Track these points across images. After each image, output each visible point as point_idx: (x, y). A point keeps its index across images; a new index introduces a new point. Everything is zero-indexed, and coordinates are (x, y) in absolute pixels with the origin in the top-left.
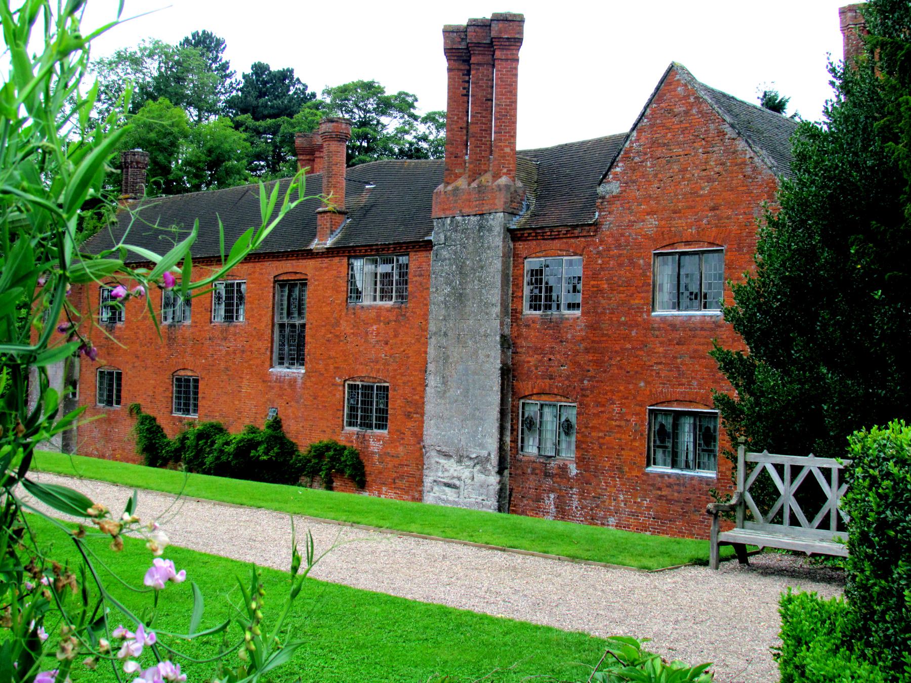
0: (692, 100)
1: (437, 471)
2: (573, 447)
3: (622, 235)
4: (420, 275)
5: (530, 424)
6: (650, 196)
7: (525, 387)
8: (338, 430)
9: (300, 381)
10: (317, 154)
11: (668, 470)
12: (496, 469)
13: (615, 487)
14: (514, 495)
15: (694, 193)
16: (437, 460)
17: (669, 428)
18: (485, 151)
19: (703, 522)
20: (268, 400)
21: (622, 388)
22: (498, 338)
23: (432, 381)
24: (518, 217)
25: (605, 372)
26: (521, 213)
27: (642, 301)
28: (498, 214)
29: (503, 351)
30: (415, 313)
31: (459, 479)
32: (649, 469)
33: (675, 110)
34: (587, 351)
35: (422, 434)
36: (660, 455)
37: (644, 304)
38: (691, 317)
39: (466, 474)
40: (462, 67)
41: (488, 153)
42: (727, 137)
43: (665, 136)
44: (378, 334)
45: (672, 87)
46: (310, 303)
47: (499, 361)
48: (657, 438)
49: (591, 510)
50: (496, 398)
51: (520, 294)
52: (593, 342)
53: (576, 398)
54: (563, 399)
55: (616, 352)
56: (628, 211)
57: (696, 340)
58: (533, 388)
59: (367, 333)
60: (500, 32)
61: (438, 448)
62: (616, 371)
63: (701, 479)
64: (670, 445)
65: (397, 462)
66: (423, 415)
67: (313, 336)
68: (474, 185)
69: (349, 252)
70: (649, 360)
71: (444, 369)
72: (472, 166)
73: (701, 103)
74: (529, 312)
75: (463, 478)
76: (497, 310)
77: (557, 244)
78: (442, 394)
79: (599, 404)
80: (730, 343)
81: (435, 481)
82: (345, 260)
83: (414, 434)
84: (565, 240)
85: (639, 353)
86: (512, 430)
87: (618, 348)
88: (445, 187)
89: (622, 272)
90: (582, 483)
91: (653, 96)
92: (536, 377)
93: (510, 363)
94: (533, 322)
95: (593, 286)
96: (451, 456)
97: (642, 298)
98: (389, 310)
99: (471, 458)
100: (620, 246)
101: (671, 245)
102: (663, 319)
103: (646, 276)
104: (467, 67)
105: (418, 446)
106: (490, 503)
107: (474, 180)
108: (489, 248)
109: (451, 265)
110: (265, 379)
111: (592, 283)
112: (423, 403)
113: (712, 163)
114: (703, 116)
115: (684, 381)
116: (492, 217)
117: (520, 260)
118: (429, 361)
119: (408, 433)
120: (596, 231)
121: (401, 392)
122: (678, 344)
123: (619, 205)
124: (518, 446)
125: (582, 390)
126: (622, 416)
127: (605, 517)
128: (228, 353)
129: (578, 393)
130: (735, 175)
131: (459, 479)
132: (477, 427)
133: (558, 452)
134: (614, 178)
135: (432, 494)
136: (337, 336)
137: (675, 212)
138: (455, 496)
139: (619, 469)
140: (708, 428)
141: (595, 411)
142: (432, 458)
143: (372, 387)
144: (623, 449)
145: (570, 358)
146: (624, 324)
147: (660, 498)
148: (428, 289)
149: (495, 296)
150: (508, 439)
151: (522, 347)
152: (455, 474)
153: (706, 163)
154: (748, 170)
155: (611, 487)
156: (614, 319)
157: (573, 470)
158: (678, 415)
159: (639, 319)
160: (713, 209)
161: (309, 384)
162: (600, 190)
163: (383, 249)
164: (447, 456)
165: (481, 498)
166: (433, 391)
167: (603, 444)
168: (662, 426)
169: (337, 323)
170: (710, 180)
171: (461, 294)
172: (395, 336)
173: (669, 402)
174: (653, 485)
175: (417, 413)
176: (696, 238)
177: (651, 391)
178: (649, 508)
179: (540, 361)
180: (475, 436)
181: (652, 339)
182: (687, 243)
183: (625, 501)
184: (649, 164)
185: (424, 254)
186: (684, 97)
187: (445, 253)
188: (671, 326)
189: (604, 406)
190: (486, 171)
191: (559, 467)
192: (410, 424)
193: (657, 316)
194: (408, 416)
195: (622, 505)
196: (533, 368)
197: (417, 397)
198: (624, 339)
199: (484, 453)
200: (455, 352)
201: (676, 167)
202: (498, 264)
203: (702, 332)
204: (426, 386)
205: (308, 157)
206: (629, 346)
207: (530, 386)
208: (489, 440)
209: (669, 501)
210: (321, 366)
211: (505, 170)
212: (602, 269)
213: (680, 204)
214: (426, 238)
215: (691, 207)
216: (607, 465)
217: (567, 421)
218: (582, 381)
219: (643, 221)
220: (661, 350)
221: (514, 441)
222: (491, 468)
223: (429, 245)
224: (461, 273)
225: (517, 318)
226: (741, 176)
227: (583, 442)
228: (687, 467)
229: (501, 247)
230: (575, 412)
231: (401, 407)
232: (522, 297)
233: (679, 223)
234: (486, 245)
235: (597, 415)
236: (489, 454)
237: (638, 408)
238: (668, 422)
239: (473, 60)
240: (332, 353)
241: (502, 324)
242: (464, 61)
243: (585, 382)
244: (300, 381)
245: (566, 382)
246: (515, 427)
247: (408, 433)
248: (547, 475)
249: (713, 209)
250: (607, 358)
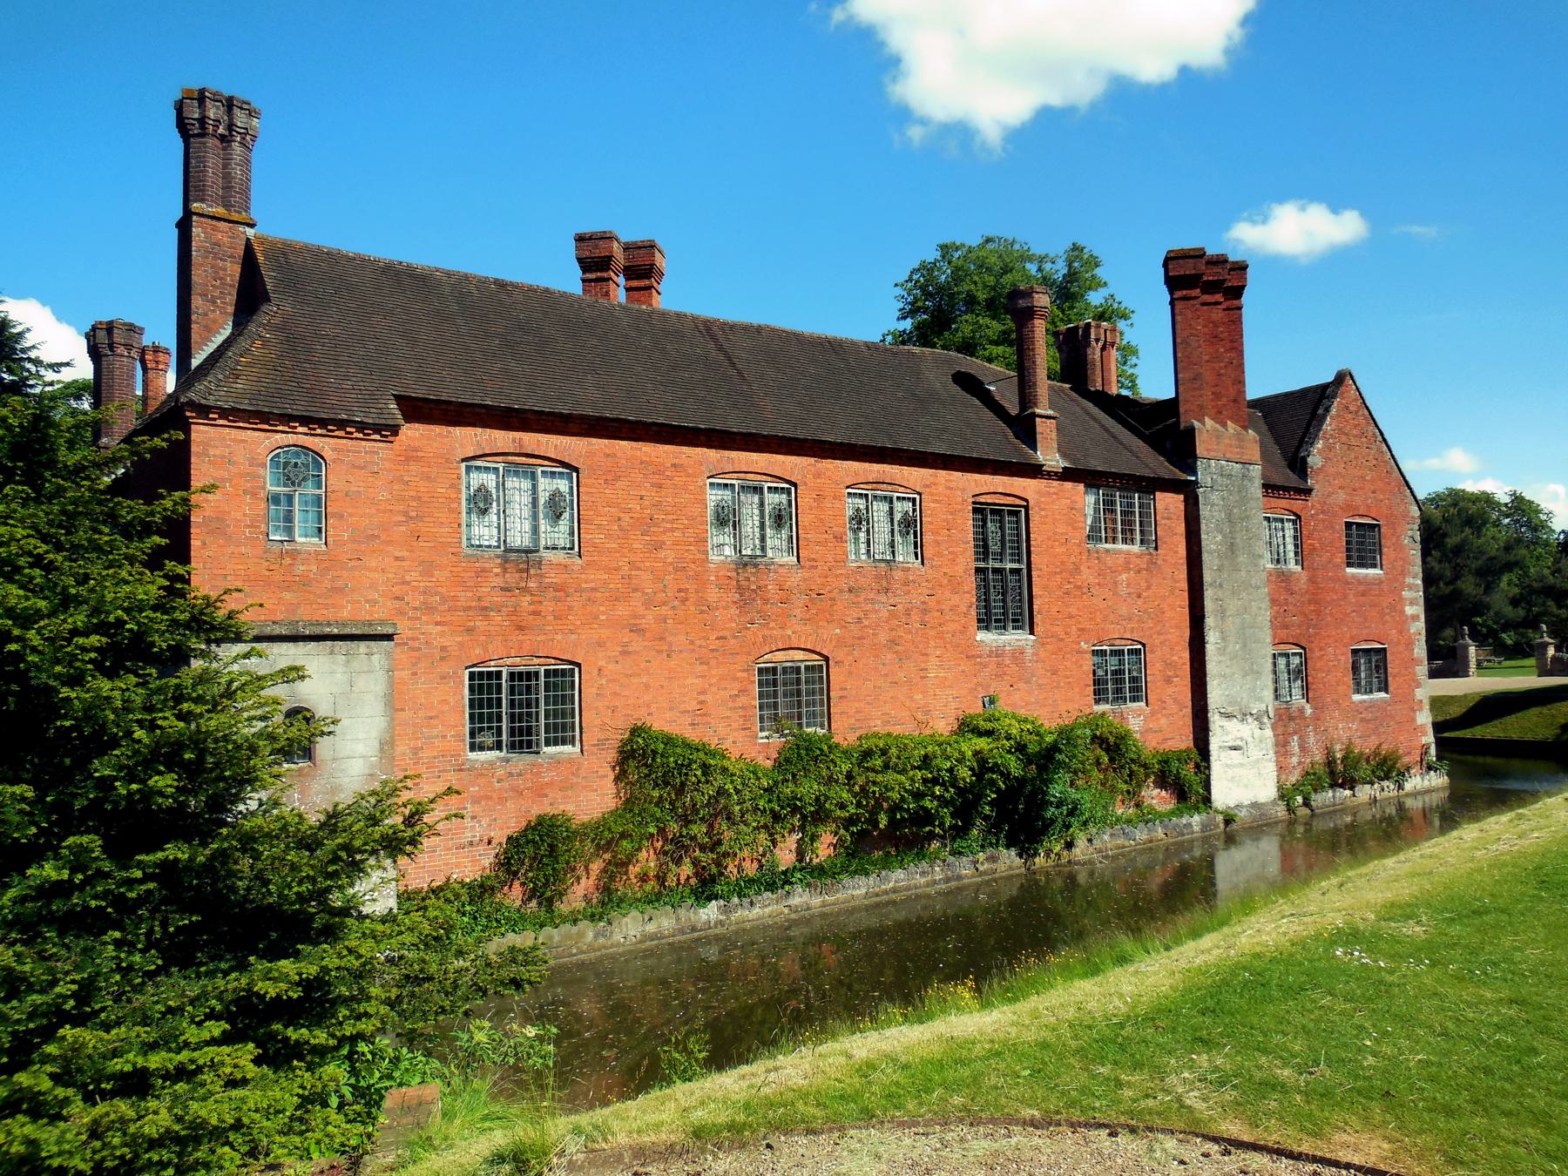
9: (1029, 651)
20: (978, 684)
44: (1128, 585)
65: (1160, 737)
67: (1045, 588)
78: (1222, 651)
98: (1139, 556)
110: (970, 653)
119: (1169, 701)
121: (1158, 653)
128: (893, 615)
136: (1079, 587)
147: (1362, 720)
161: (1042, 654)
164: (1229, 716)
169: (1077, 569)
172: (1149, 588)
192: (1170, 690)
200: (1232, 605)
209: (1367, 721)
210: (1059, 630)
233: (1358, 500)
240: (1073, 611)
244: (1029, 651)
247: (1169, 701)
248: (1291, 718)
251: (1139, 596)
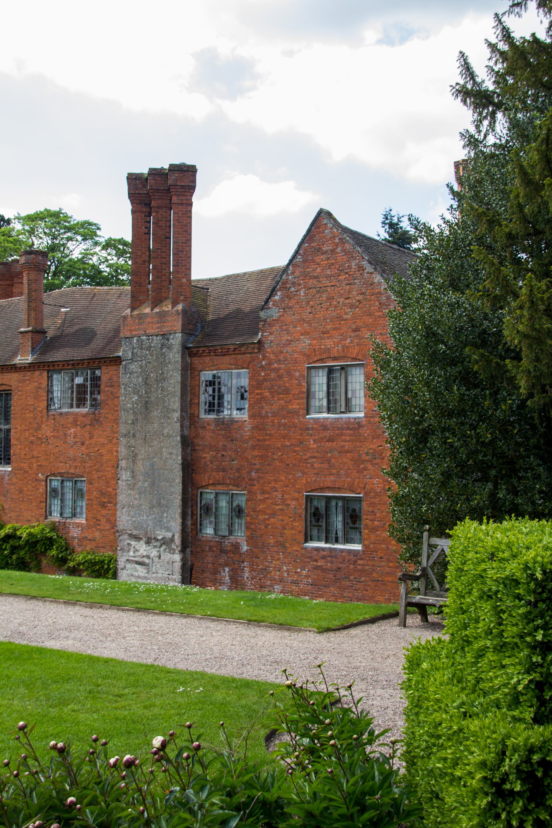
0: (337, 240)
1: (129, 551)
2: (243, 528)
3: (282, 352)
4: (110, 386)
5: (207, 509)
6: (303, 320)
7: (203, 478)
8: (42, 519)
10: (16, 280)
11: (322, 545)
12: (179, 548)
13: (279, 559)
14: (195, 568)
15: (340, 318)
16: (129, 542)
17: (323, 511)
18: (165, 281)
19: (352, 587)
21: (283, 478)
22: (179, 438)
23: (125, 476)
24: (193, 337)
25: (269, 465)
26: (196, 333)
27: (298, 407)
28: (177, 335)
29: (183, 449)
30: (107, 418)
31: (148, 557)
32: (307, 544)
33: (323, 249)
34: (253, 448)
35: (115, 520)
36: (315, 532)
37: (300, 409)
38: (338, 419)
39: (154, 553)
40: (144, 209)
41: (167, 282)
42: (366, 271)
43: (314, 270)
45: (321, 229)
46: (14, 410)
47: (180, 458)
48: (313, 519)
49: (260, 579)
50: (178, 488)
51: (197, 401)
52: (258, 440)
53: (246, 487)
54: (234, 488)
55: (278, 448)
56: (285, 332)
57: (343, 438)
58: (209, 479)
59: (65, 435)
60: (176, 181)
61: (130, 532)
62: (278, 464)
63: (350, 551)
64: (324, 525)
65: (94, 544)
66: (115, 504)
67: (18, 439)
68: (157, 310)
69: (49, 366)
70: (305, 455)
71: (133, 465)
72: (154, 294)
73: (344, 244)
74: (204, 417)
75: (152, 556)
76: (177, 415)
77: (227, 359)
78: (132, 487)
79: (264, 492)
80: (371, 440)
81: (128, 560)
82: (45, 374)
83: (108, 520)
84: (233, 356)
85: (296, 449)
86: (192, 515)
87: (279, 445)
88: (132, 311)
89: (281, 383)
90: (252, 558)
91: (305, 236)
92: (212, 471)
93: (189, 458)
94: (208, 424)
95: (258, 394)
96: (140, 539)
97: (298, 404)
98: (85, 415)
99: (158, 540)
100: (279, 360)
101: (321, 360)
102: (316, 420)
103: (302, 385)
104: (148, 210)
105: (112, 530)
106: (174, 577)
107: (156, 306)
108: (169, 363)
109: (138, 377)
111: (257, 391)
112: (116, 494)
113: (353, 293)
114: (346, 254)
115: (334, 471)
116: (172, 337)
117: (197, 373)
118: (120, 458)
119: (103, 520)
120: (259, 349)
122: (328, 441)
123: (278, 328)
124: (197, 528)
125: (250, 480)
126: (284, 500)
127: (271, 586)
129: (247, 483)
130: (373, 302)
131: (148, 557)
132: (163, 513)
133: (231, 532)
134: (273, 305)
135: (124, 571)
136: (39, 439)
137: (324, 333)
138: (145, 571)
139: (282, 545)
140: (354, 510)
141: (261, 498)
142: (125, 540)
144: (285, 529)
145: (239, 454)
146: (285, 425)
147: (316, 568)
148: (118, 397)
149: (175, 403)
150: (189, 523)
151: (199, 445)
152: (145, 554)
153: (349, 292)
155: (276, 560)
156: (276, 421)
157: (245, 548)
158: (329, 499)
159: (296, 421)
160: (355, 330)
161: (14, 480)
162: (262, 314)
163: (78, 364)
164: (137, 538)
165: (167, 573)
166: (124, 483)
167: (269, 525)
168: (317, 509)
169: (39, 428)
170: (352, 306)
171: (147, 402)
172: (91, 438)
173: (322, 489)
174: (310, 557)
175: (111, 503)
176: (342, 354)
177: (307, 480)
178: (307, 577)
179: (215, 457)
180: (162, 521)
181: (307, 437)
182: (335, 359)
183: (288, 571)
184: (302, 294)
185: (114, 368)
186: (331, 238)
187: (134, 367)
188: (323, 425)
189: (269, 493)
190: (166, 298)
191: (232, 545)
192: (104, 512)
193: (310, 419)
194: (103, 505)
195: (286, 575)
196: (209, 463)
197: (111, 489)
198: (284, 438)
199: (169, 535)
200: (142, 452)
201: (325, 296)
202: (177, 377)
203: (348, 431)
204: (119, 479)
205: (8, 282)
206: (288, 443)
207: (206, 478)
208: (173, 524)
210: (25, 466)
211: (182, 298)
212: (265, 380)
213: (328, 327)
214: (116, 355)
215: (336, 329)
216: (272, 541)
217: (238, 506)
218: (249, 472)
219: (298, 340)
220: (315, 446)
221: (194, 524)
222: (175, 547)
223: (118, 361)
224: (146, 383)
225: (195, 422)
226: (377, 304)
227: (251, 523)
228: (337, 541)
229: (180, 362)
230: (244, 499)
231: (97, 498)
232: (199, 403)
233: (329, 343)
234: (167, 361)
235: (263, 501)
236: (173, 536)
237: (296, 495)
238: (322, 505)
239: (153, 204)
240: (35, 453)
241: (182, 426)
242: (146, 204)
243: (253, 474)
245: (237, 474)
246: (195, 512)
247: (103, 520)
248: (222, 551)
249: (355, 330)
250: (270, 454)
251: (83, 444)
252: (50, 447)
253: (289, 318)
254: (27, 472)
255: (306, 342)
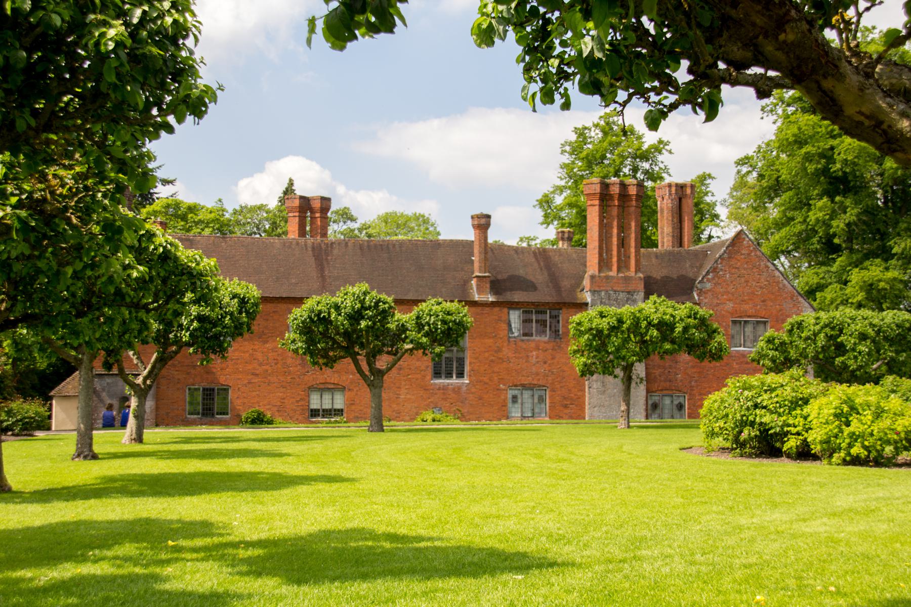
9: (464, 388)
15: (753, 293)
101: (741, 317)
143: (213, 390)
153: (759, 279)
154: (781, 285)
160: (763, 301)
170: (761, 288)
182: (749, 317)
201: (743, 280)
210: (485, 379)
218: (690, 382)
233: (746, 307)
240: (496, 369)
243: (693, 383)
244: (464, 388)
251: (545, 363)
252: (511, 365)
253: (719, 289)
254: (487, 383)
255: (730, 306)
